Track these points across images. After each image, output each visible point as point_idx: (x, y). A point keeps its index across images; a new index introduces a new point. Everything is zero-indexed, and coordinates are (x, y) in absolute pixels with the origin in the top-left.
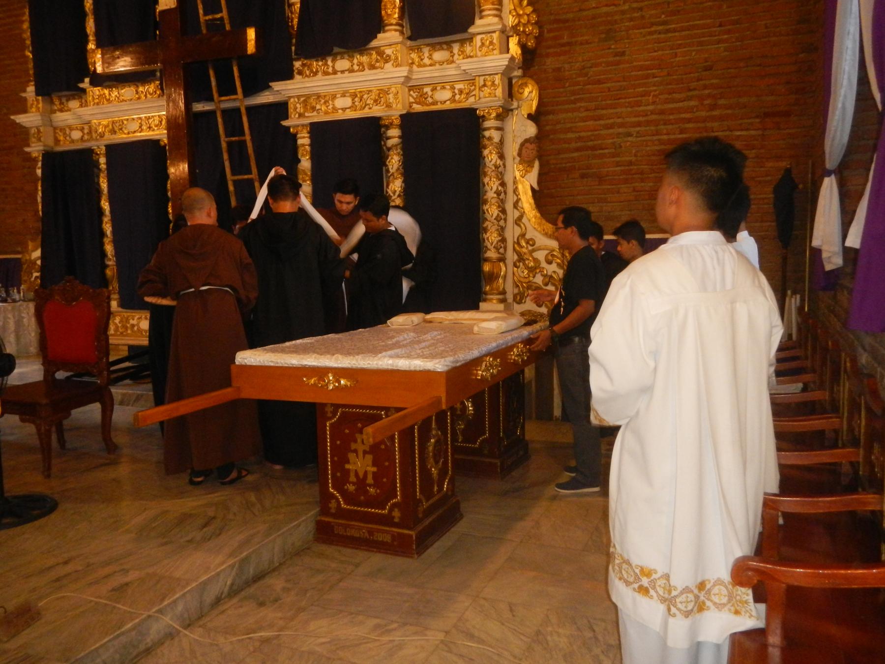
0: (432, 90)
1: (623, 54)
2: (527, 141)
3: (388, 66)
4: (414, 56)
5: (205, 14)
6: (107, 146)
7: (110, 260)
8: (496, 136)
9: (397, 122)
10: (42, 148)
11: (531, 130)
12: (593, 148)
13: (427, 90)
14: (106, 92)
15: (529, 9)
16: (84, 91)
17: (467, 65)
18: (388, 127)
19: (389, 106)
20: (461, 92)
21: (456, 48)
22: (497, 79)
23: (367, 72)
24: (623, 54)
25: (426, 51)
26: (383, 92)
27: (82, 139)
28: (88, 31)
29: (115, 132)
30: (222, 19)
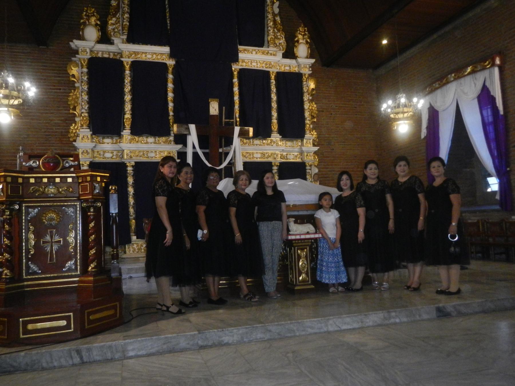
0: (287, 154)
1: (333, 149)
2: (315, 174)
3: (275, 145)
4: (281, 143)
5: (225, 119)
6: (136, 163)
7: (131, 216)
8: (310, 171)
9: (278, 164)
10: (91, 160)
11: (316, 170)
14: (136, 138)
15: (316, 133)
16: (120, 136)
17: (304, 149)
18: (272, 166)
19: (275, 158)
20: (296, 156)
21: (295, 142)
22: (312, 154)
23: (266, 146)
24: (333, 149)
25: (284, 142)
26: (272, 154)
27: (112, 158)
28: (126, 109)
29: (140, 156)
30: (233, 122)
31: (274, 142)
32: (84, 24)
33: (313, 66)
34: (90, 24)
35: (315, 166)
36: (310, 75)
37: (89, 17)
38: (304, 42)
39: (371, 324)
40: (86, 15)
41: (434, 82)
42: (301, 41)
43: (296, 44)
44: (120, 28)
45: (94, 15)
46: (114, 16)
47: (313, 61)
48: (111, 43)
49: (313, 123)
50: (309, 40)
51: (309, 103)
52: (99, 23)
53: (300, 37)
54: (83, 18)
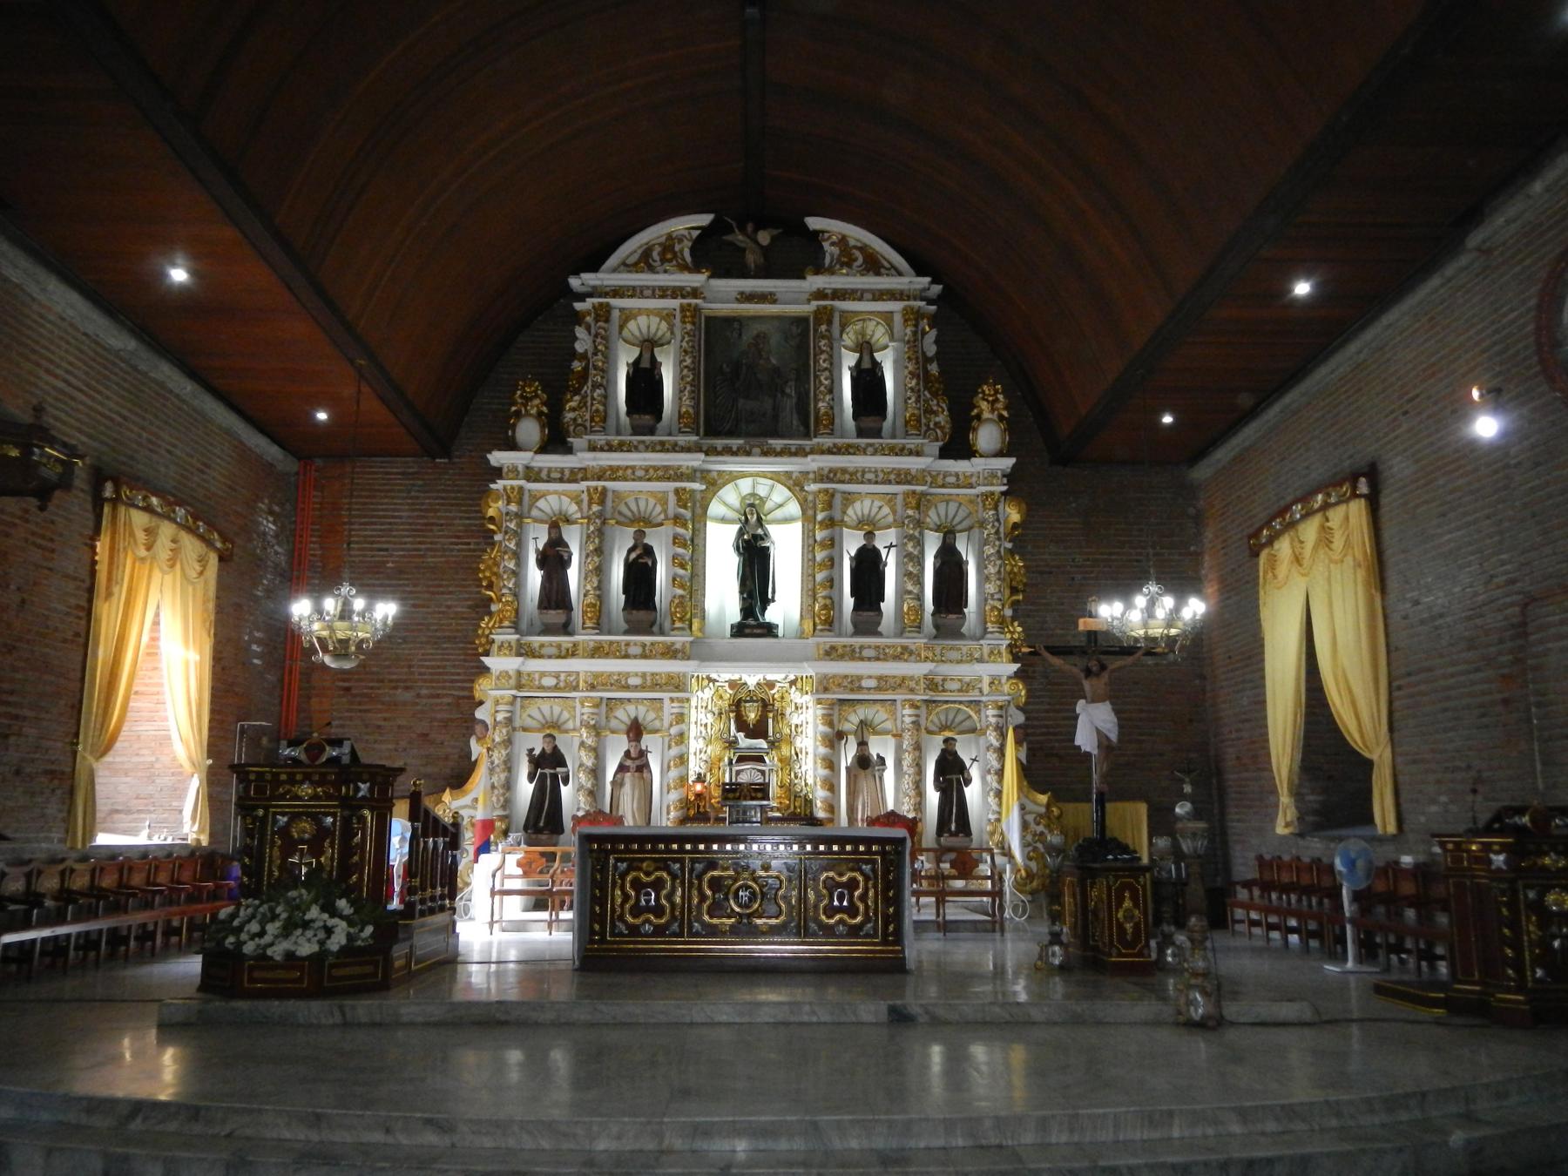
12: (1055, 734)
13: (938, 679)
26: (904, 679)
31: (911, 653)
32: (518, 415)
33: (1011, 477)
34: (528, 414)
35: (1018, 708)
36: (1003, 493)
37: (527, 400)
38: (995, 416)
39: (767, 1019)
40: (522, 396)
41: (1273, 518)
42: (986, 415)
43: (975, 423)
44: (588, 417)
45: (537, 396)
46: (577, 392)
47: (1008, 463)
48: (568, 450)
49: (1015, 604)
50: (1005, 414)
51: (1000, 558)
52: (545, 409)
53: (984, 405)
54: (515, 404)
